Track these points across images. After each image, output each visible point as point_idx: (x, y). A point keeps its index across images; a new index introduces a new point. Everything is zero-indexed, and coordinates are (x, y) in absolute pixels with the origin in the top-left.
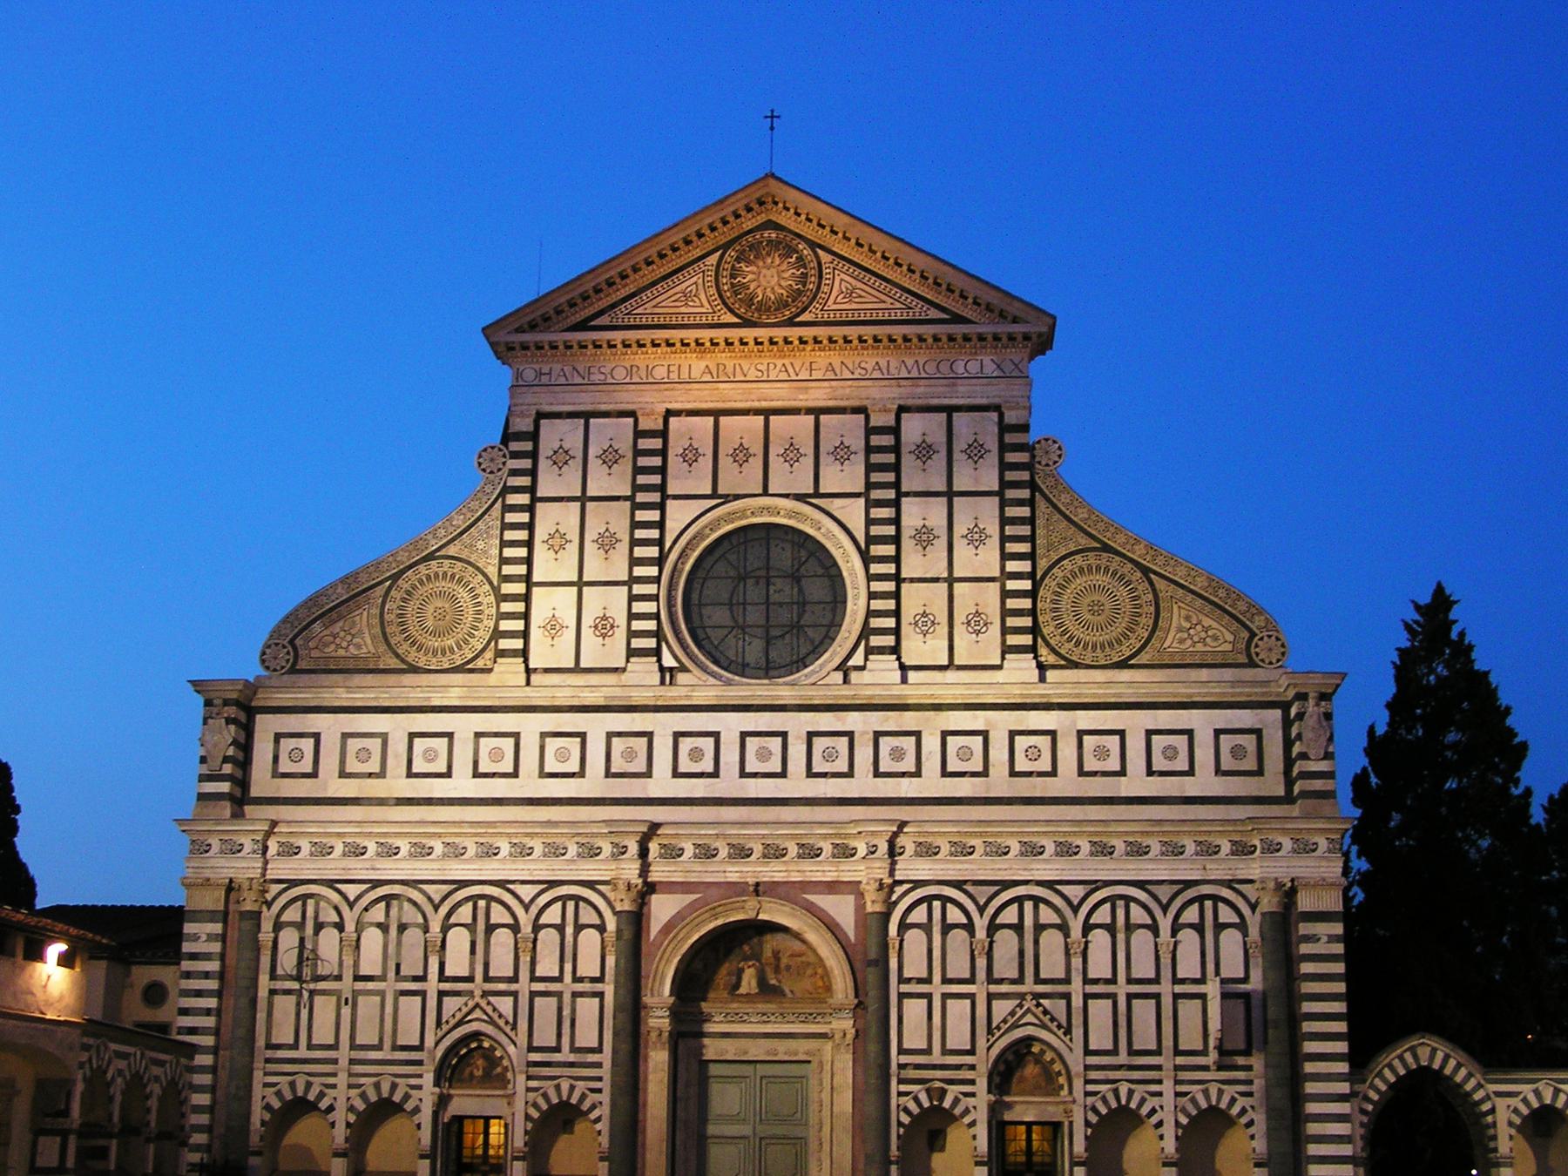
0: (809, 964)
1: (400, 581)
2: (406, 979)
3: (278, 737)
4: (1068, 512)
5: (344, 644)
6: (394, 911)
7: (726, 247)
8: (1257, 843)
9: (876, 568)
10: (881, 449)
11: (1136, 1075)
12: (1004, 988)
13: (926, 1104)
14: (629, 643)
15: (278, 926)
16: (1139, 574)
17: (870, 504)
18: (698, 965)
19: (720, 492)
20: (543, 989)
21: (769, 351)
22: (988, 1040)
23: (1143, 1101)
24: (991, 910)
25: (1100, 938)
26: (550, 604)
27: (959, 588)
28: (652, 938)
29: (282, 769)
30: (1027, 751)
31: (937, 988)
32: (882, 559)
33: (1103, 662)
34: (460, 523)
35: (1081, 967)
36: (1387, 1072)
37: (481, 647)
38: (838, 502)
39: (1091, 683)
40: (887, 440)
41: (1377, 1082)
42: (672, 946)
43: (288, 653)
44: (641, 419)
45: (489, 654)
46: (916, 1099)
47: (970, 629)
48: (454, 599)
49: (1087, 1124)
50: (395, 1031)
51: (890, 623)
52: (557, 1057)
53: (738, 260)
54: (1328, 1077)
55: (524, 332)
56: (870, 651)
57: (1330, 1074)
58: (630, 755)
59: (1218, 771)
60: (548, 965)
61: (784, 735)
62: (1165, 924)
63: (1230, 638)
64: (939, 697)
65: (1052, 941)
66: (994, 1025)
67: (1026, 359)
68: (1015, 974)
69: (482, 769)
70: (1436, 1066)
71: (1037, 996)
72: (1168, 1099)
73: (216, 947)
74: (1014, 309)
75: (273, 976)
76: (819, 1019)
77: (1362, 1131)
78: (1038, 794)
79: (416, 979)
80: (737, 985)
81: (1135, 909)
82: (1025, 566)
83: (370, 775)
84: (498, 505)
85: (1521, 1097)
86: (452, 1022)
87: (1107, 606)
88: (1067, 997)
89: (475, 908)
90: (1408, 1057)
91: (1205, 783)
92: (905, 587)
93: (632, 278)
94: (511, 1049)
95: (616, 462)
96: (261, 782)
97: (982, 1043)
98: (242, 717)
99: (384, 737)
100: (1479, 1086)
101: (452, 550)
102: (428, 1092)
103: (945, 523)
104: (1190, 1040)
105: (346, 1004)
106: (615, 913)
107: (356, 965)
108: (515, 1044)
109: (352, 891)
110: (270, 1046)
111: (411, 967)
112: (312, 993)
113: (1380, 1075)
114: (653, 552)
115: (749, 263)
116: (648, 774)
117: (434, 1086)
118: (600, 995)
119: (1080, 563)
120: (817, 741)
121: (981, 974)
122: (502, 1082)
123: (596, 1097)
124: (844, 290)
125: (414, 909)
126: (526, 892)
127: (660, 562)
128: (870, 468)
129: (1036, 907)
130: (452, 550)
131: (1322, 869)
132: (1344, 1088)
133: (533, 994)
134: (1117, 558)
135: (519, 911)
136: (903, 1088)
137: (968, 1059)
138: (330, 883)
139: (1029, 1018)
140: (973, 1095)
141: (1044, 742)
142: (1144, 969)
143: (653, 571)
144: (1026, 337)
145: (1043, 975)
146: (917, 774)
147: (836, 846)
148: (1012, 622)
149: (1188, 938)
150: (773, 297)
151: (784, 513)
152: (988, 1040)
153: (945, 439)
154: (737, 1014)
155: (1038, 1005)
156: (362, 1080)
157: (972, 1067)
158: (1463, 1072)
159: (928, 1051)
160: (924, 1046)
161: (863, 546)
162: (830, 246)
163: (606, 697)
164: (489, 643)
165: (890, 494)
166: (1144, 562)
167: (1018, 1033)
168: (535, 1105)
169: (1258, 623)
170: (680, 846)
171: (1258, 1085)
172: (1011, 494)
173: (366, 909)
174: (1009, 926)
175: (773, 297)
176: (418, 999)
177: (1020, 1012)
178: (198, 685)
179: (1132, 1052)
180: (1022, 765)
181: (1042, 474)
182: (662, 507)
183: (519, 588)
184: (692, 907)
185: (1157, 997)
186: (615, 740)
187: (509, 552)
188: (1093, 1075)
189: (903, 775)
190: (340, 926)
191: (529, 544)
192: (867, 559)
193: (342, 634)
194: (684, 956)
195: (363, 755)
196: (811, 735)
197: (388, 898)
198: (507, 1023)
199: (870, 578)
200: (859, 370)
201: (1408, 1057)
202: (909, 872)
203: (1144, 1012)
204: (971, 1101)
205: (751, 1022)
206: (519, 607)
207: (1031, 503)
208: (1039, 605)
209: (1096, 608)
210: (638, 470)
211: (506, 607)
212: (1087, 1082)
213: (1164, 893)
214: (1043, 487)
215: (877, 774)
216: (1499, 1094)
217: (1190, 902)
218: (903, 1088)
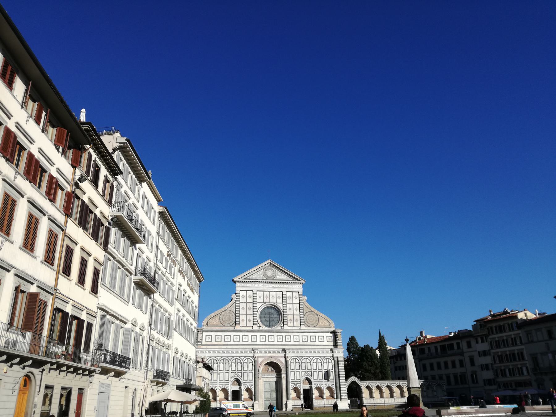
1: (222, 313)
2: (226, 371)
3: (206, 336)
6: (224, 361)
7: (264, 269)
12: (303, 371)
17: (283, 304)
19: (264, 302)
24: (301, 360)
25: (315, 364)
27: (294, 316)
31: (295, 371)
32: (285, 312)
41: (348, 383)
46: (293, 386)
48: (229, 316)
50: (225, 378)
52: (247, 381)
58: (254, 338)
59: (327, 342)
60: (245, 368)
61: (274, 336)
62: (322, 362)
68: (304, 369)
69: (235, 340)
74: (301, 280)
77: (347, 389)
78: (305, 344)
79: (228, 371)
80: (268, 370)
81: (319, 360)
82: (302, 313)
84: (235, 303)
88: (311, 372)
90: (352, 379)
91: (326, 343)
94: (241, 380)
96: (204, 343)
97: (301, 378)
99: (221, 336)
101: (229, 309)
103: (292, 307)
109: (218, 358)
112: (213, 373)
113: (349, 382)
114: (256, 310)
115: (267, 271)
116: (257, 341)
118: (253, 372)
121: (301, 369)
126: (242, 358)
127: (257, 311)
130: (229, 309)
132: (345, 384)
135: (241, 361)
136: (292, 384)
137: (300, 380)
138: (216, 357)
139: (307, 375)
140: (300, 385)
141: (306, 337)
143: (256, 313)
144: (302, 283)
145: (308, 369)
146: (291, 341)
149: (325, 364)
153: (292, 296)
156: (221, 385)
157: (300, 381)
158: (358, 381)
160: (294, 379)
165: (286, 303)
167: (306, 377)
168: (244, 388)
174: (303, 362)
176: (228, 373)
179: (319, 379)
180: (303, 340)
182: (256, 304)
184: (264, 359)
190: (217, 363)
192: (283, 312)
196: (277, 336)
197: (223, 359)
201: (352, 379)
204: (300, 386)
215: (286, 341)
217: (325, 359)
218: (292, 384)
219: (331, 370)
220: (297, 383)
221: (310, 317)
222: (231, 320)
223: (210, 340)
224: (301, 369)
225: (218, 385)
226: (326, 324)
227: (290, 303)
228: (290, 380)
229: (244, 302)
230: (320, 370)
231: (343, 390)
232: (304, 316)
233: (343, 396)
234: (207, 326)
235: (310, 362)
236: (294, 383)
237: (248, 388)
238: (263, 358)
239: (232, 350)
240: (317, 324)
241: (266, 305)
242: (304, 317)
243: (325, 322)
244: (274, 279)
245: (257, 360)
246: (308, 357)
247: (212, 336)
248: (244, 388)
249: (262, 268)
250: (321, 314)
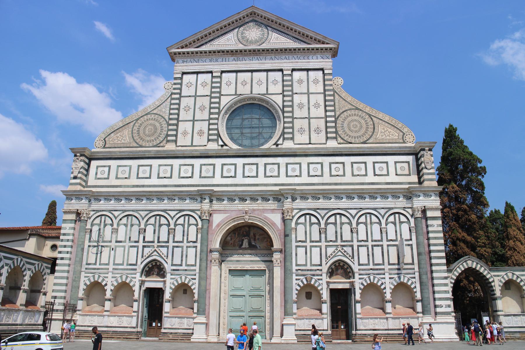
0: (265, 238)
1: (138, 121)
2: (132, 242)
3: (97, 167)
4: (345, 98)
5: (120, 140)
8: (411, 195)
9: (286, 115)
10: (287, 81)
11: (376, 272)
12: (331, 243)
13: (305, 283)
14: (208, 138)
15: (92, 225)
16: (368, 116)
17: (284, 96)
18: (229, 238)
20: (177, 245)
21: (253, 54)
22: (326, 261)
23: (379, 280)
25: (362, 228)
28: (213, 228)
29: (98, 177)
30: (335, 169)
31: (308, 244)
33: (358, 142)
34: (158, 104)
35: (356, 236)
36: (458, 269)
37: (162, 140)
40: (289, 78)
41: (455, 273)
42: (220, 231)
43: (103, 142)
44: (213, 73)
45: (165, 142)
46: (302, 281)
47: (315, 132)
48: (155, 126)
49: (360, 289)
50: (128, 259)
51: (291, 130)
53: (244, 30)
54: (440, 271)
55: (179, 48)
56: (284, 139)
57: (441, 270)
58: (207, 171)
59: (396, 175)
62: (383, 222)
63: (397, 135)
64: (307, 152)
66: (328, 256)
67: (330, 56)
68: (334, 239)
72: (387, 280)
73: (72, 231)
75: (90, 241)
76: (269, 255)
77: (451, 289)
78: (339, 182)
79: (136, 242)
80: (242, 245)
82: (332, 114)
83: (126, 178)
84: (170, 98)
85: (502, 276)
86: (147, 256)
87: (358, 126)
88: (352, 246)
89: (156, 219)
90: (464, 264)
91: (392, 178)
92: (295, 120)
93: (212, 34)
94: (165, 265)
95: (206, 86)
96: (92, 180)
97: (324, 262)
98: (87, 161)
99: (130, 167)
101: (155, 112)
103: (307, 102)
104: (394, 260)
105: (113, 250)
106: (202, 220)
107: (117, 237)
108: (167, 264)
109: (116, 214)
110: (87, 264)
111: (134, 238)
114: (217, 111)
115: (247, 31)
117: (140, 277)
118: (196, 247)
119: (349, 113)
120: (267, 166)
121: (323, 239)
123: (194, 281)
124: (275, 37)
125: (136, 219)
127: (219, 113)
128: (283, 86)
129: (341, 217)
131: (433, 203)
132: (446, 275)
133: (174, 247)
134: (361, 112)
136: (298, 277)
137: (320, 268)
138: (110, 211)
139: (340, 253)
140: (321, 279)
141: (341, 166)
143: (217, 116)
144: (331, 49)
145: (344, 239)
147: (274, 198)
148: (329, 130)
149: (391, 227)
150: (254, 40)
152: (326, 261)
153: (306, 78)
154: (241, 254)
155: (343, 249)
157: (321, 270)
159: (306, 265)
161: (282, 109)
162: (271, 26)
163: (200, 154)
164: (165, 138)
165: (290, 93)
166: (369, 113)
168: (173, 284)
169: (405, 130)
170: (223, 199)
171: (417, 274)
172: (327, 93)
173: (121, 219)
174: (332, 223)
175: (254, 40)
176: (136, 248)
177: (336, 251)
178: (72, 149)
179: (374, 264)
180: (334, 172)
181: (336, 88)
182: (219, 98)
183: (175, 122)
185: (382, 246)
186: (203, 167)
187: (172, 111)
188: (362, 272)
189: (296, 176)
190: (112, 225)
191: (178, 109)
192: (283, 112)
193: (120, 136)
194: (224, 234)
195: (123, 172)
196: (266, 164)
198: (165, 256)
199: (284, 117)
200: (280, 59)
201: (464, 264)
202: (298, 206)
204: (320, 282)
205: (247, 257)
206: (175, 127)
207: (333, 95)
208: (337, 125)
209: (355, 126)
210: (212, 87)
211: (170, 127)
213: (382, 212)
214: (337, 91)
215: (287, 176)
216: (495, 276)
218: (298, 277)
219: (406, 240)
220: (314, 275)
221: (353, 121)
222: (156, 135)
223: (106, 176)
224: (323, 239)
225: (110, 275)
226: (393, 135)
227: (301, 93)
228: (294, 268)
229: (190, 96)
230: (376, 241)
232: (336, 119)
233: (441, 306)
234: (104, 147)
235: (348, 223)
237: (182, 283)
238: (226, 213)
239: (149, 196)
240: (371, 137)
241: (240, 101)
243: (389, 132)
245: (208, 218)
246: (345, 209)
247: (109, 167)
248: (173, 284)
249: (236, 24)
250: (380, 116)
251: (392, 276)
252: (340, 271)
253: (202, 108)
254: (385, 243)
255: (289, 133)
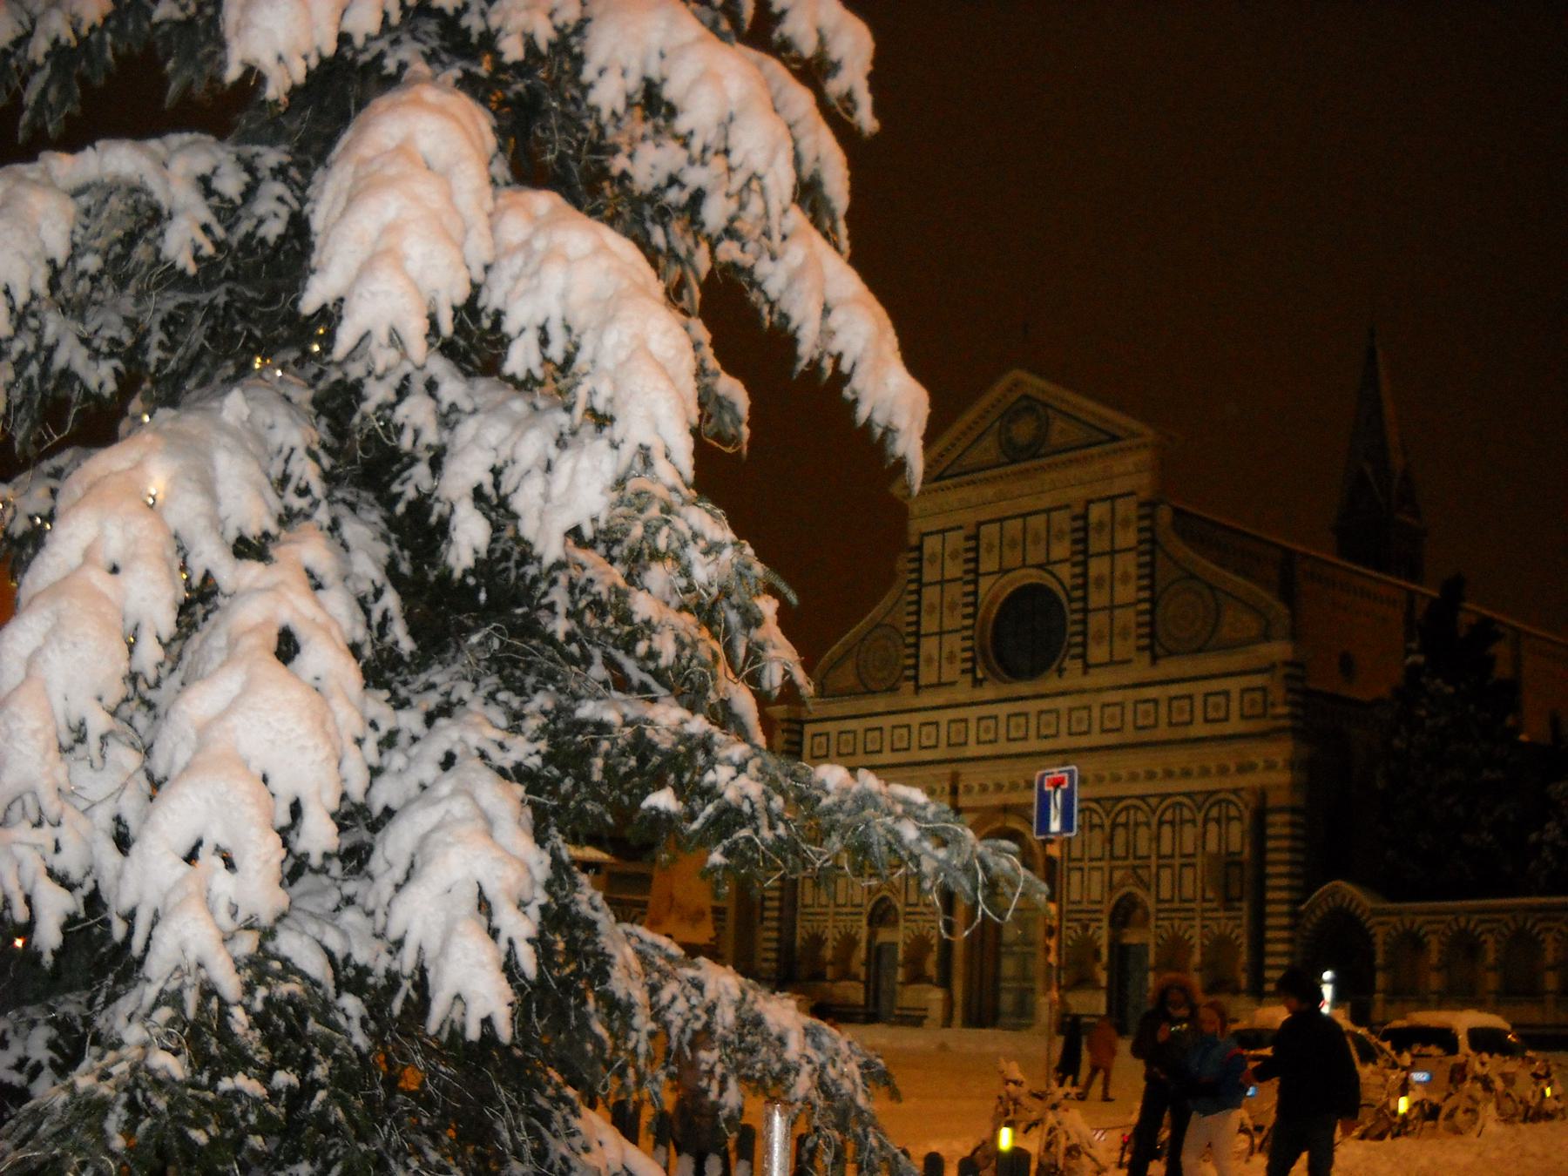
11: (1182, 915)
12: (1120, 863)
13: (1079, 931)
24: (1112, 815)
25: (1166, 830)
26: (929, 646)
31: (1086, 865)
38: (1058, 566)
39: (1186, 666)
40: (1079, 523)
56: (1073, 657)
65: (1143, 831)
70: (1345, 905)
71: (1134, 868)
72: (1197, 930)
91: (1235, 725)
92: (1090, 616)
94: (899, 906)
98: (796, 727)
100: (1369, 919)
101: (887, 620)
102: (863, 933)
110: (805, 906)
114: (970, 610)
122: (895, 923)
128: (1075, 542)
129: (1135, 814)
136: (1070, 924)
140: (1100, 928)
142: (1189, 849)
143: (969, 622)
149: (1213, 827)
151: (1033, 577)
159: (1080, 902)
167: (1125, 890)
171: (1245, 920)
180: (1140, 722)
183: (911, 640)
188: (1162, 915)
191: (918, 613)
192: (1071, 600)
203: (1188, 874)
212: (1157, 919)
213: (1199, 799)
217: (1212, 806)
225: (830, 924)
231: (1274, 954)
236: (1076, 920)
242: (1152, 612)
244: (1043, 451)
246: (1142, 798)
251: (1208, 923)
252: (1139, 912)
253: (953, 607)
254: (1198, 860)
255: (1076, 645)
